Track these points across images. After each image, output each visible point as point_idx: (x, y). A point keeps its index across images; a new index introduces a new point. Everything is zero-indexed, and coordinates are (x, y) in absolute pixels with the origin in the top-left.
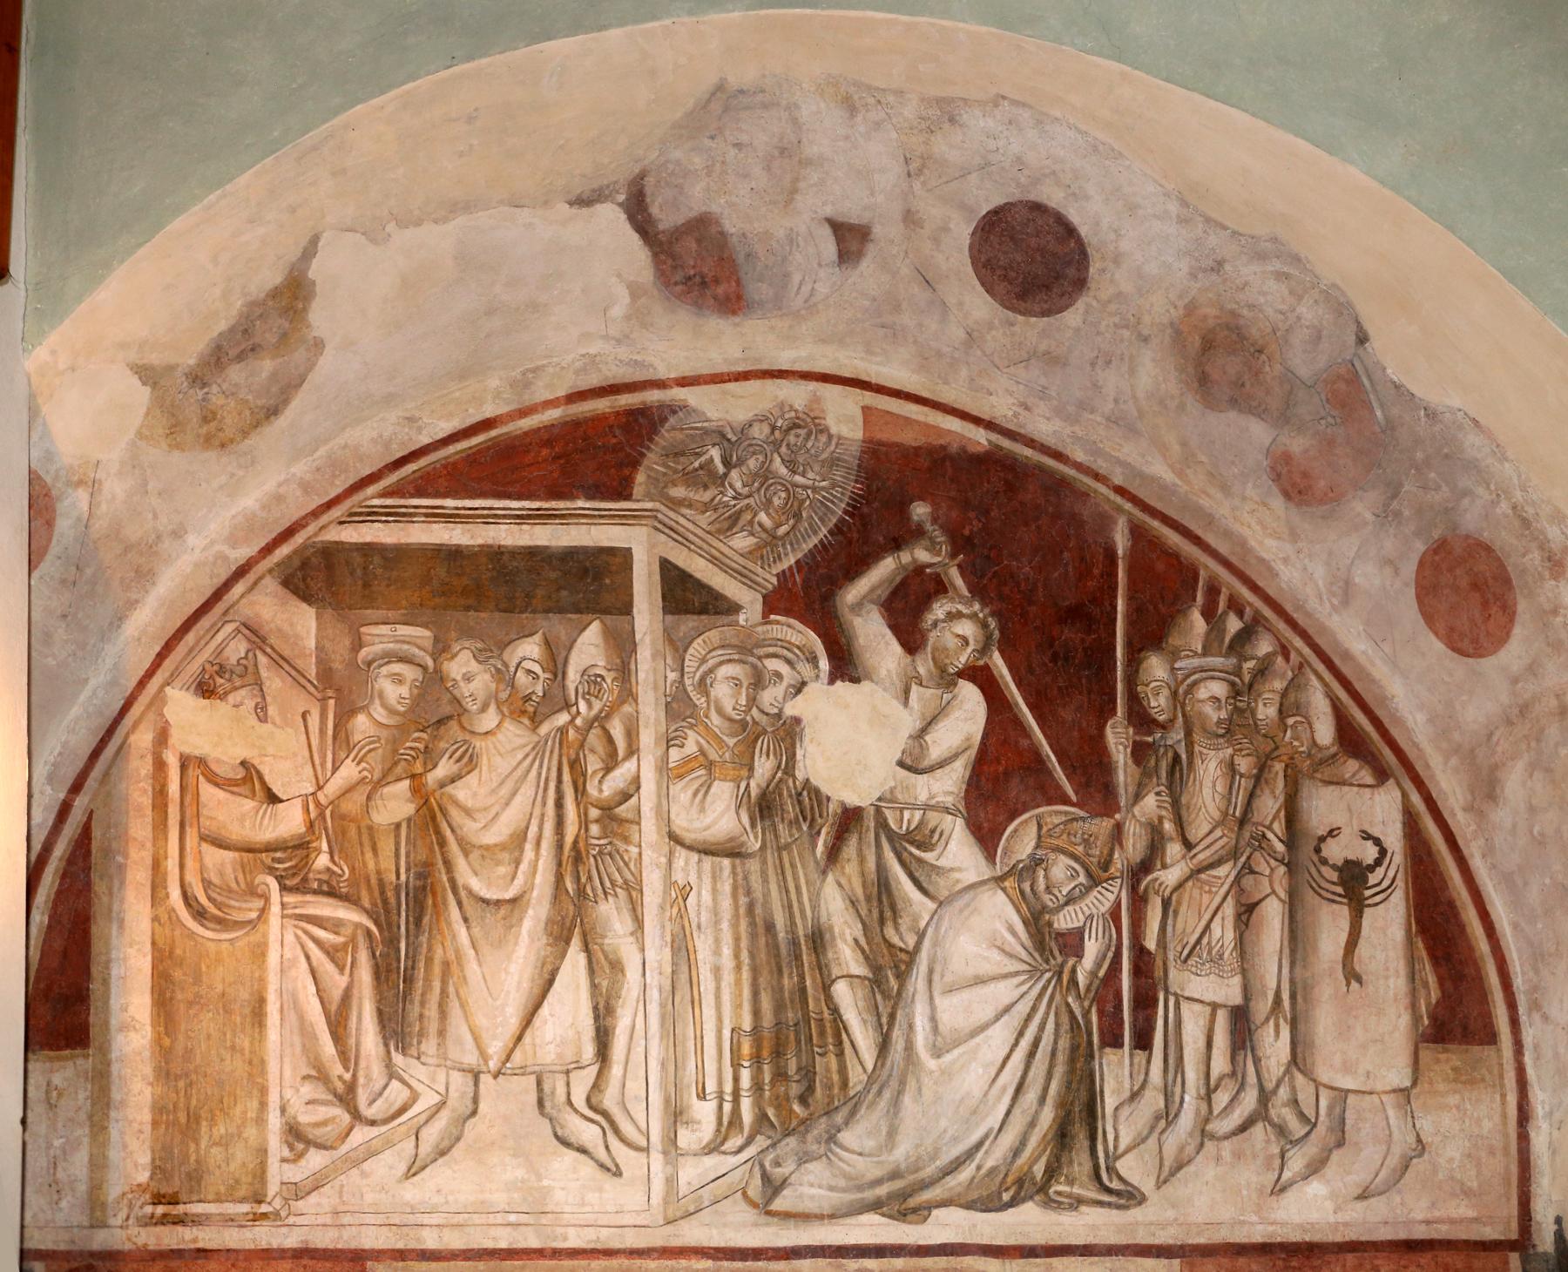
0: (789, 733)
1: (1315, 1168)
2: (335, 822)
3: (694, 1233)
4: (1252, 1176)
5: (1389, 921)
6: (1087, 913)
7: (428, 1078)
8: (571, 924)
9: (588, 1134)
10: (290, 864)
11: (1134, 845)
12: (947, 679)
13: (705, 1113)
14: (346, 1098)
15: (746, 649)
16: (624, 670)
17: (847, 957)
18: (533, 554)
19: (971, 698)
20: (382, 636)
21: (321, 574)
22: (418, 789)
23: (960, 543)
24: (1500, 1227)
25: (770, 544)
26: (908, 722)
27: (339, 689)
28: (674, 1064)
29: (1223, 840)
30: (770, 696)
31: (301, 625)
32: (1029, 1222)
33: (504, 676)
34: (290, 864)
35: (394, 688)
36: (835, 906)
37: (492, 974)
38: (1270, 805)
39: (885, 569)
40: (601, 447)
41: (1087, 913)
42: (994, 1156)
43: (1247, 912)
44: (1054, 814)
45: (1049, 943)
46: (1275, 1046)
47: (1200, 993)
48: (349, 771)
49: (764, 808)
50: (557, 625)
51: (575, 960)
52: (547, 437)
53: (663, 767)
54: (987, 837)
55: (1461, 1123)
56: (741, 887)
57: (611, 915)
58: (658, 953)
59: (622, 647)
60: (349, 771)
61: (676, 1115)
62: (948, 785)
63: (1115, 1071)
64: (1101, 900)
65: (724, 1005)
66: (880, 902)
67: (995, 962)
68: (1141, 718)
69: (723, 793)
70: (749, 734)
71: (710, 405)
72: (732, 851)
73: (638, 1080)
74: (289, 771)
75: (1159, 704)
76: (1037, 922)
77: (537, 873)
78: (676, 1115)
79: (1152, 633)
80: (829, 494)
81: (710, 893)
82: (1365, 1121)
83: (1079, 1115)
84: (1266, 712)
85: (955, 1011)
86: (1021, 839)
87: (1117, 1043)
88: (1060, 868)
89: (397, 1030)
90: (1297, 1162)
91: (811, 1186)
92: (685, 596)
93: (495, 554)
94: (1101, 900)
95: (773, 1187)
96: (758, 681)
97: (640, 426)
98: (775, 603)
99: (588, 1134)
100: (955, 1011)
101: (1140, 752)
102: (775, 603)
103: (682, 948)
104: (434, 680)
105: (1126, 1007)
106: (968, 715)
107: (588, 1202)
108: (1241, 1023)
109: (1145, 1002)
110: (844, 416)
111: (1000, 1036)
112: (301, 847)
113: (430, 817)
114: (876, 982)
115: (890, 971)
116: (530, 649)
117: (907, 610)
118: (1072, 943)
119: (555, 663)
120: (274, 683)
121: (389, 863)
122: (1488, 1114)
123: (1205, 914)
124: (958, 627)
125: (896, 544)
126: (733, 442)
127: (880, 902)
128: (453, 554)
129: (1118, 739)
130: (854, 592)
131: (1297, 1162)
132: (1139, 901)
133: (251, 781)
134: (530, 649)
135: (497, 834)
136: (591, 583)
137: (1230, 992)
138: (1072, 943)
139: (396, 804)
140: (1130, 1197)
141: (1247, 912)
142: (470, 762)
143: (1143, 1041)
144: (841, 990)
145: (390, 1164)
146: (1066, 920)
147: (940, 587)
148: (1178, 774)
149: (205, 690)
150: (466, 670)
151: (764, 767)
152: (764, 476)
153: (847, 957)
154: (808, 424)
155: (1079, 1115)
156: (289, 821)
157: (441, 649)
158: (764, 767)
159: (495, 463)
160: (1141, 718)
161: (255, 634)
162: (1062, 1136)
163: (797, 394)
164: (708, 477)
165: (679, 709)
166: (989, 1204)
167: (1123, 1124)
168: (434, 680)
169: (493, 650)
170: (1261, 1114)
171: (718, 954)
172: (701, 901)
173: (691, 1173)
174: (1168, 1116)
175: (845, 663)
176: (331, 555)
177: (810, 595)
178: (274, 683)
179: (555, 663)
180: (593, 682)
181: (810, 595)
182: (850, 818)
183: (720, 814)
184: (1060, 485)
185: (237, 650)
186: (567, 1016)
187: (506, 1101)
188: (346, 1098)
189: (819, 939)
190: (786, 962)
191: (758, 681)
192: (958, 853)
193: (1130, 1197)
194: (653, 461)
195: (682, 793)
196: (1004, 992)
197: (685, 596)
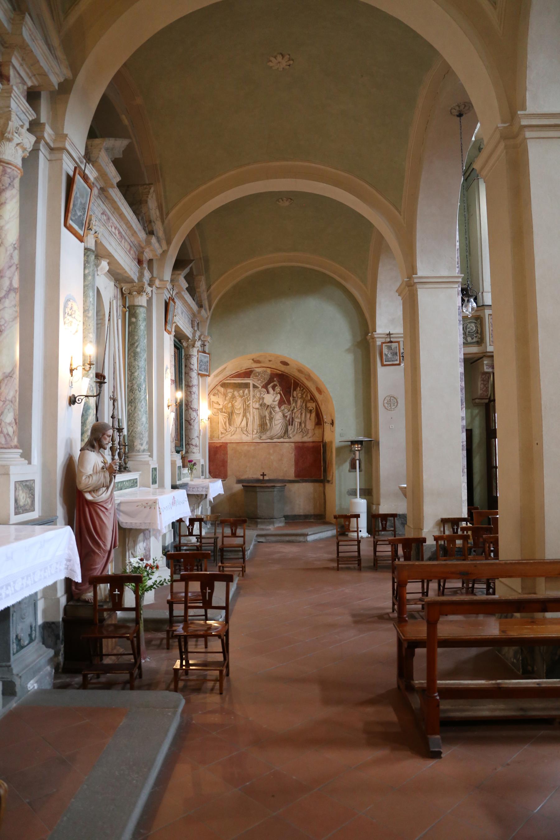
0: (263, 398)
1: (306, 435)
2: (225, 406)
3: (254, 441)
4: (300, 436)
5: (314, 415)
6: (288, 414)
7: (232, 429)
8: (245, 415)
9: (245, 433)
10: (221, 410)
11: (292, 408)
12: (277, 394)
13: (255, 431)
14: (226, 430)
15: (260, 391)
16: (249, 393)
17: (268, 418)
18: (242, 383)
19: (279, 395)
20: (229, 390)
21: (224, 385)
22: (232, 404)
23: (278, 382)
24: (321, 440)
25: (262, 382)
26: (273, 397)
27: (225, 395)
28: (253, 427)
29: (300, 408)
30: (262, 395)
31: (222, 390)
32: (282, 440)
33: (239, 394)
34: (221, 410)
35: (230, 395)
36: (267, 413)
37: (238, 419)
38: (304, 404)
39: (272, 384)
40: (248, 374)
41: (288, 414)
42: (279, 435)
43: (301, 414)
44: (286, 405)
45: (285, 416)
46: (303, 425)
47: (297, 421)
48: (226, 402)
49: (261, 405)
50: (244, 389)
51: (245, 418)
52: (243, 373)
53: (253, 402)
54: (280, 407)
55: (318, 432)
56: (259, 412)
57: (248, 414)
58: (252, 418)
59: (249, 391)
60: (226, 402)
61: (253, 431)
62: (276, 403)
63: (290, 428)
64: (289, 413)
65: (257, 422)
66: (271, 413)
67: (280, 418)
68: (293, 397)
69: (257, 404)
70: (260, 399)
71: (257, 370)
72: (258, 409)
73: (250, 428)
74: (221, 403)
75: (295, 396)
76: (284, 415)
77: (242, 411)
78: (253, 431)
79: (295, 389)
80: (267, 377)
81: (256, 412)
82: (310, 432)
83: (286, 431)
84: (304, 396)
85: (276, 422)
86: (283, 408)
87: (289, 425)
88: (286, 410)
89: (230, 424)
90: (304, 435)
91: (264, 437)
92: (255, 387)
93: (239, 383)
94: (289, 413)
95: (261, 437)
96: (261, 394)
97: (251, 372)
98: (263, 387)
99: (245, 433)
100: (276, 422)
101: (293, 400)
102: (263, 387)
103: (254, 417)
104: (233, 394)
105: (291, 422)
106: (278, 397)
107: (246, 438)
108: (300, 423)
109: (292, 422)
110: (269, 371)
111: (280, 425)
112: (222, 409)
113: (233, 406)
114: (270, 420)
115: (271, 419)
116: (241, 391)
117: (274, 388)
118: (287, 417)
119: (243, 393)
120: (220, 394)
121: (229, 410)
122: (321, 431)
123: (298, 414)
124: (278, 389)
125: (273, 382)
126: (259, 373)
127: (271, 413)
128: (235, 383)
129: (291, 399)
130: (269, 386)
131: (304, 435)
132: (292, 413)
133: (218, 403)
134: (241, 391)
135: (239, 407)
136: (247, 386)
137: (300, 421)
138: (287, 417)
139: (230, 405)
140: (290, 438)
141: (301, 414)
142: (236, 401)
143: (292, 425)
144: (267, 421)
145: (229, 435)
146: (286, 415)
147: (277, 385)
148: (296, 402)
149: (214, 395)
150: (236, 393)
151: (261, 401)
152: (262, 376)
153: (268, 418)
154: (266, 371)
155: (286, 431)
156: (221, 407)
157: (234, 391)
158: (261, 401)
159: (239, 375)
160: (293, 397)
161: (218, 391)
162: (285, 433)
163: (264, 369)
164: (257, 376)
165: (254, 396)
166: (279, 439)
167: (290, 432)
168: (233, 394)
169: (238, 391)
170: (302, 431)
171: (257, 418)
172: (255, 413)
173: (254, 436)
174: (294, 431)
175: (268, 392)
176: (224, 383)
177: (265, 386)
178: (220, 394)
179: (243, 393)
180: (247, 394)
181: (265, 386)
182: (268, 406)
183: (257, 406)
184: (287, 377)
185: (217, 392)
186: (244, 422)
187: (239, 430)
188: (226, 430)
189: (265, 416)
190: (262, 418)
191: (261, 394)
192: (277, 409)
193: (290, 438)
194: (252, 375)
195: (254, 404)
196: (280, 421)
197: (255, 387)
